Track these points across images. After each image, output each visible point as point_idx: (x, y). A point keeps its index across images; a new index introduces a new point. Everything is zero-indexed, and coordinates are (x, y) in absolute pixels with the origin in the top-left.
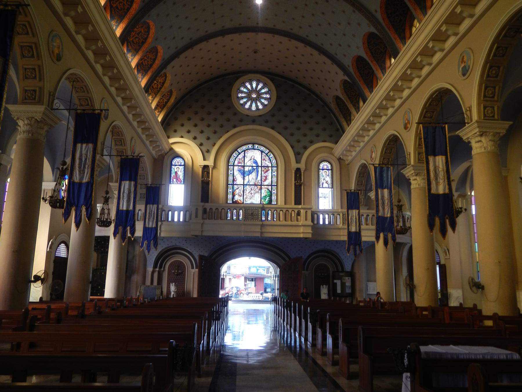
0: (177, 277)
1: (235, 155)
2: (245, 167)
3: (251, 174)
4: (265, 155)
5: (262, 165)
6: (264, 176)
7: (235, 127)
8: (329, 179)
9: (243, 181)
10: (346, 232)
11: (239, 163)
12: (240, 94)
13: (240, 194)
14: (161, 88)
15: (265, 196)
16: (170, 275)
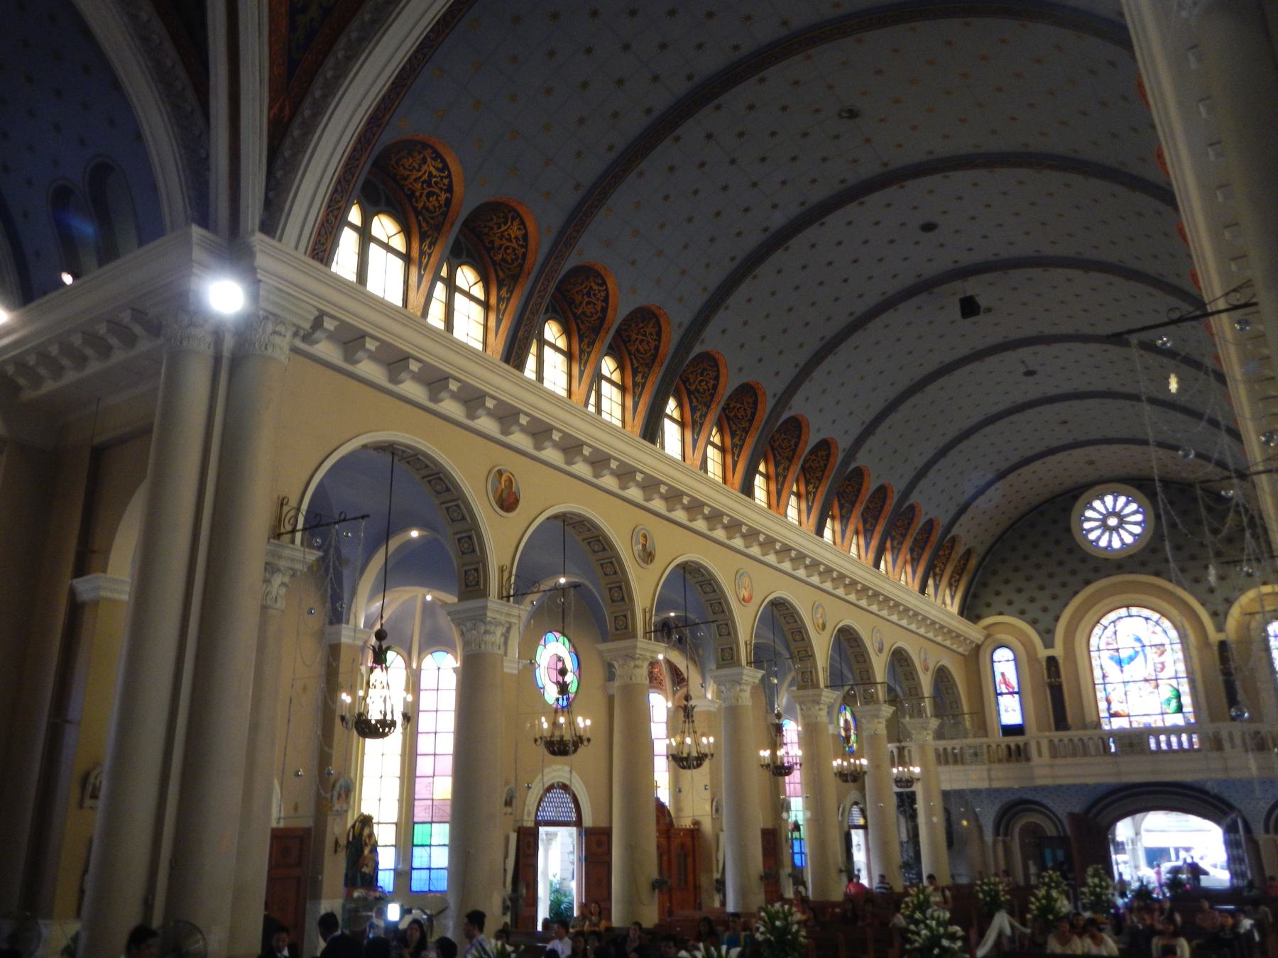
7: (1087, 583)
11: (1108, 644)
14: (950, 554)
15: (1169, 700)
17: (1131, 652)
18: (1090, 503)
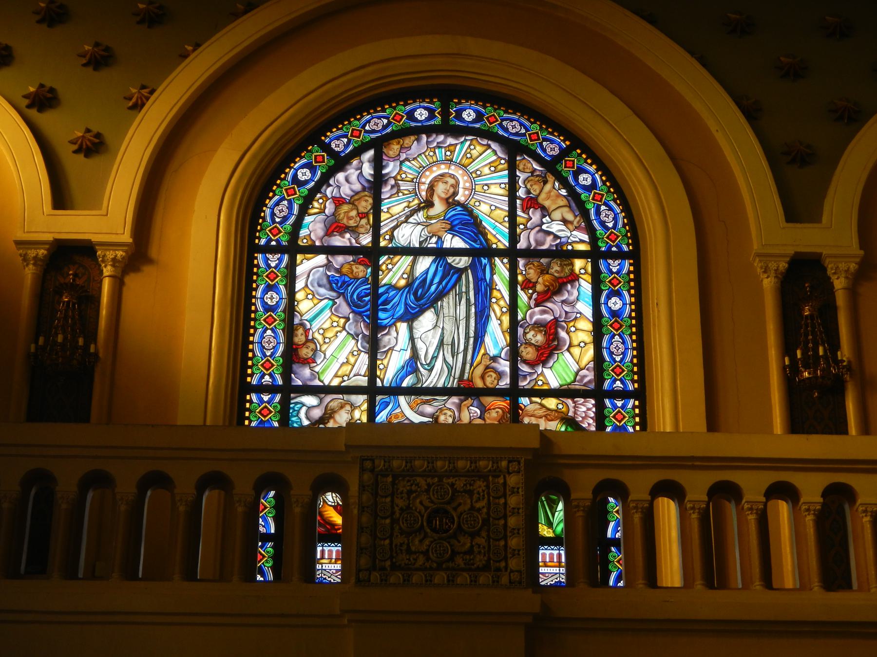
1: (304, 175)
2: (383, 259)
5: (522, 245)
6: (539, 326)
9: (364, 358)
11: (334, 227)
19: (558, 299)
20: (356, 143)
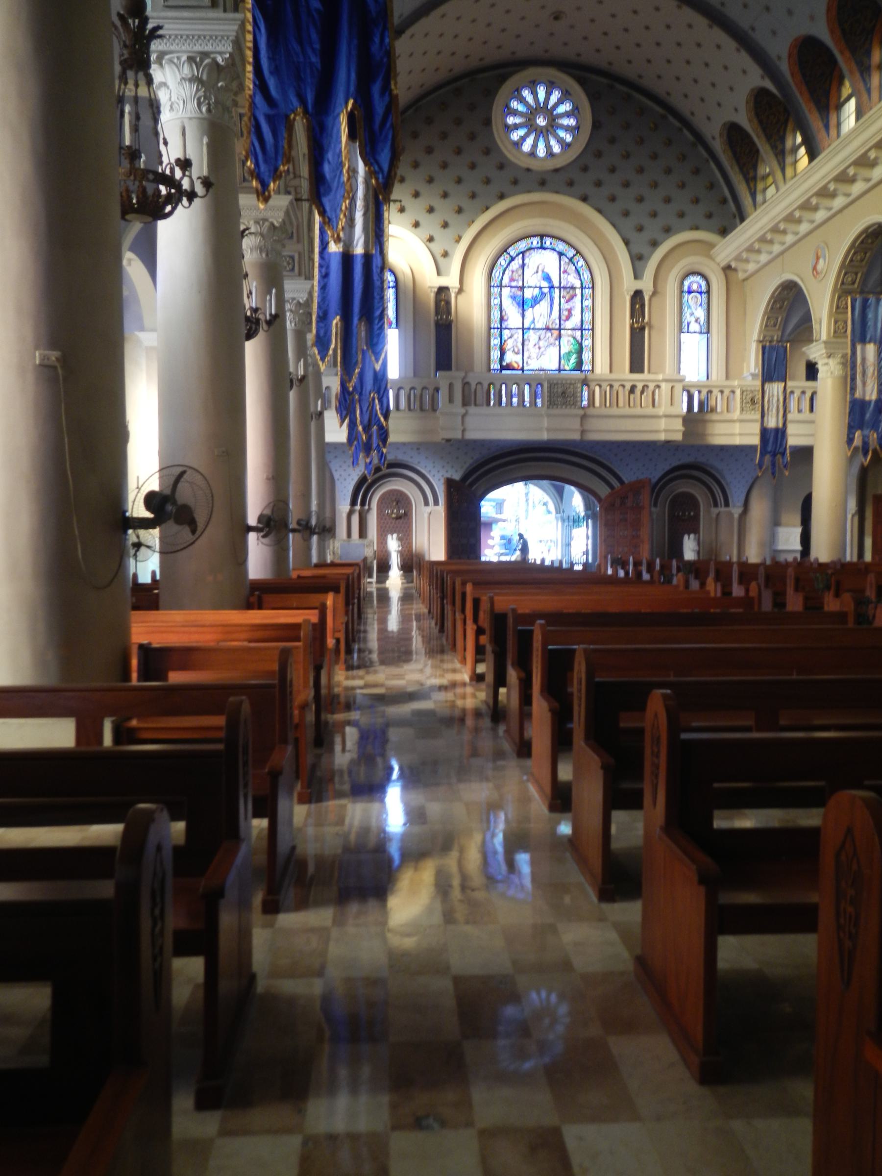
0: (395, 523)
2: (525, 289)
3: (538, 306)
4: (567, 260)
5: (562, 285)
6: (567, 309)
7: (502, 197)
8: (701, 313)
10: (756, 429)
11: (512, 280)
12: (512, 118)
13: (516, 350)
15: (569, 354)
16: (382, 519)
17: (536, 291)
18: (518, 90)
19: (572, 301)
20: (517, 251)
